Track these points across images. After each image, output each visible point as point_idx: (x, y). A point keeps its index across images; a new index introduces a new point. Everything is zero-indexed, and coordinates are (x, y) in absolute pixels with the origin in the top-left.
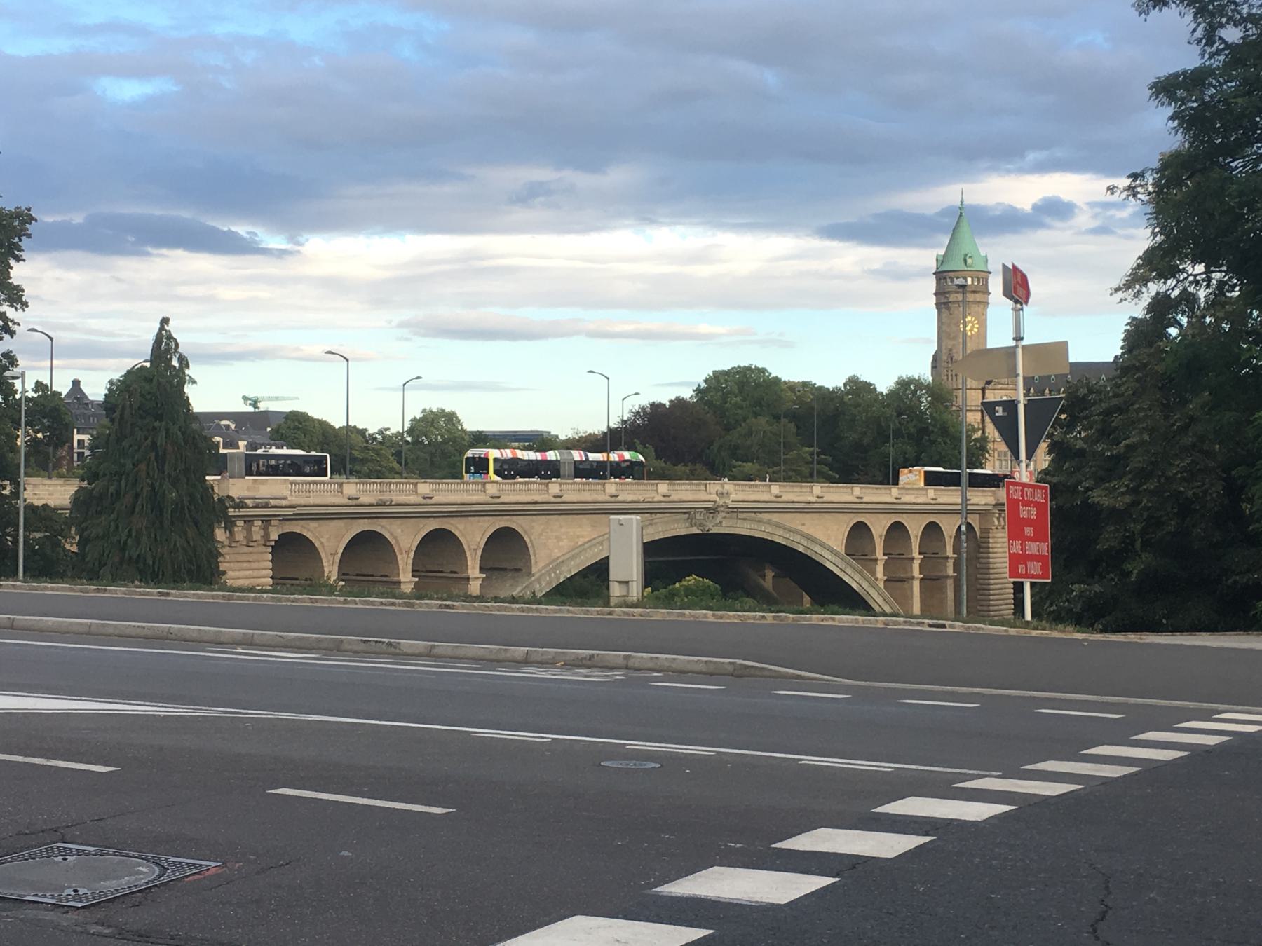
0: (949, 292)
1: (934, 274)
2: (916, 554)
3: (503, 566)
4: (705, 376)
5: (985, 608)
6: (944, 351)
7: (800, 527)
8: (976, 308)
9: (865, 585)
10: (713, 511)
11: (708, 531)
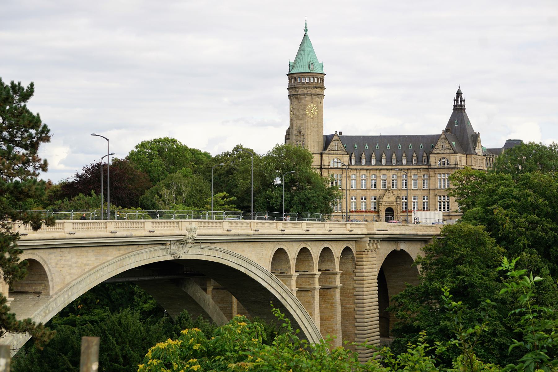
0: (298, 88)
1: (287, 75)
2: (316, 272)
3: (27, 289)
4: (137, 144)
5: (361, 309)
6: (295, 128)
7: (241, 253)
8: (317, 99)
9: (284, 295)
10: (182, 243)
11: (179, 258)
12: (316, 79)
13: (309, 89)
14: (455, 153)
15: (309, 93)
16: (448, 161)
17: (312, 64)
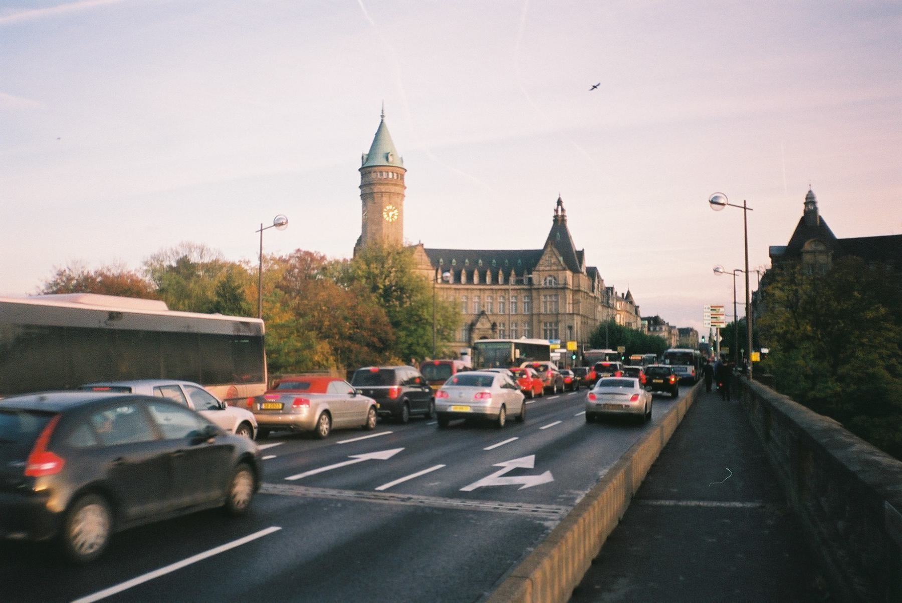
8: (396, 199)
12: (395, 175)
13: (387, 187)
14: (564, 269)
15: (387, 191)
16: (555, 279)
17: (391, 155)
